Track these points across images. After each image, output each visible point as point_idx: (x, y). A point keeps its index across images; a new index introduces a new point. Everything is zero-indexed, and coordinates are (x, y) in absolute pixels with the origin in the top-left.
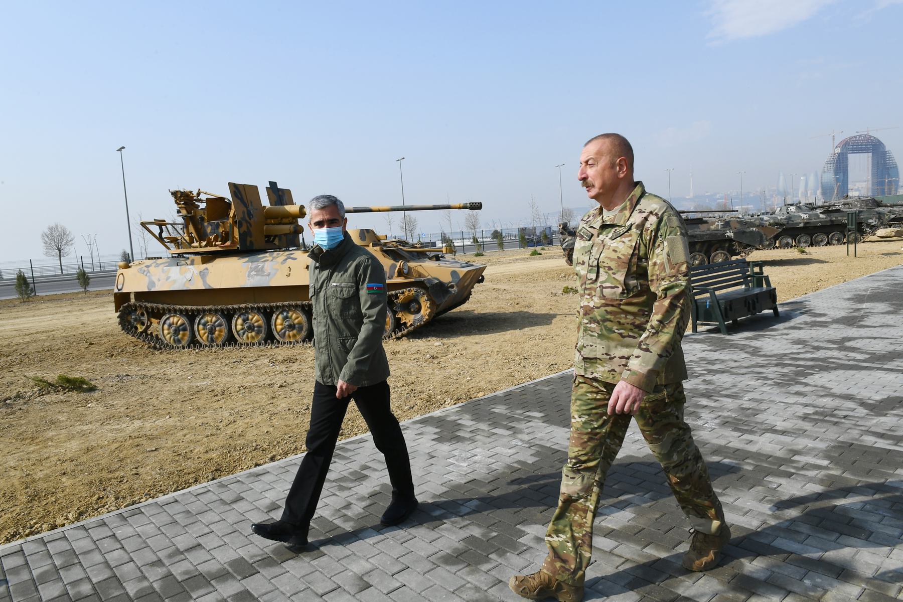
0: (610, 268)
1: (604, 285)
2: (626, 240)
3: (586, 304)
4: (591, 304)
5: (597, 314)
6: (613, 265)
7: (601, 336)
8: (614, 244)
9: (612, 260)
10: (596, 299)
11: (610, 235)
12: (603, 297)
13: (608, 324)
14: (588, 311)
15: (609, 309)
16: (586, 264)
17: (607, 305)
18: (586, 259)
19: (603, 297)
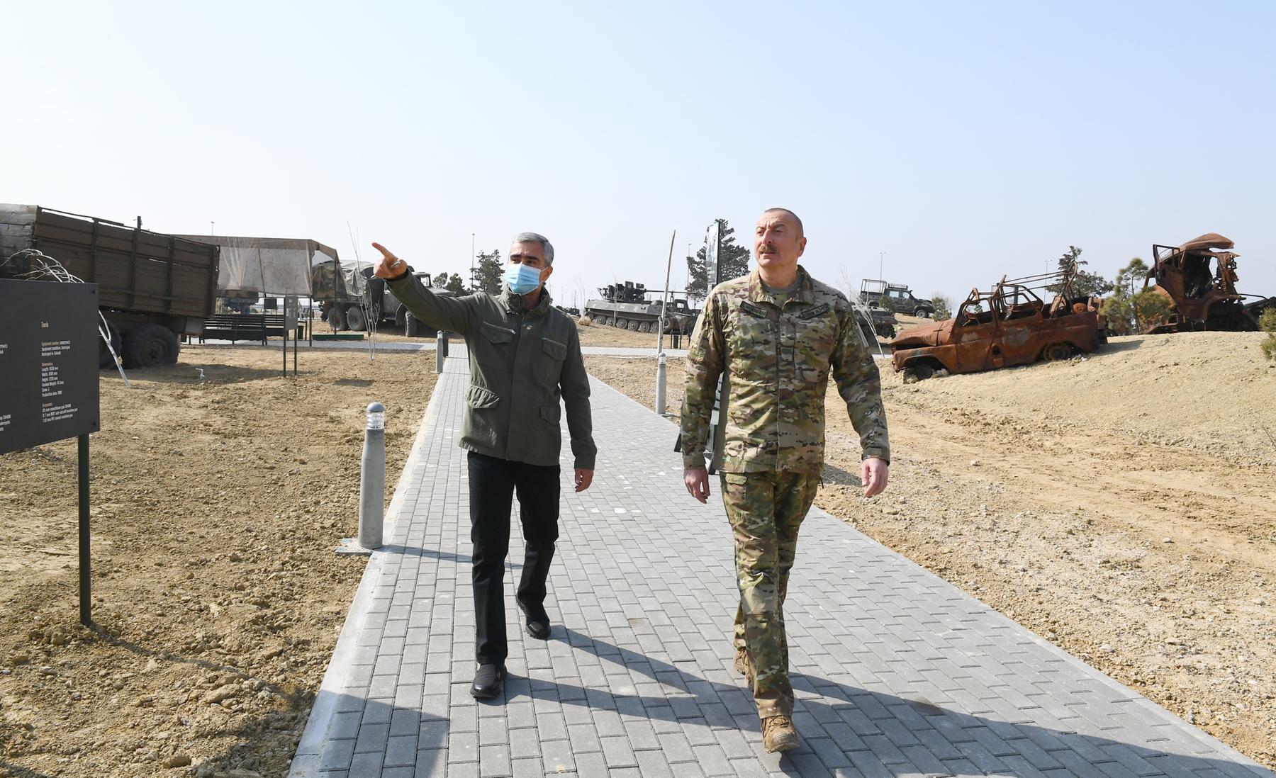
0: (812, 349)
1: (804, 367)
2: (826, 320)
3: (782, 387)
4: (791, 388)
5: (796, 399)
6: (816, 345)
7: (795, 423)
8: (812, 324)
9: (814, 340)
10: (796, 382)
11: (798, 314)
12: (803, 379)
13: (806, 408)
14: (784, 396)
15: (809, 392)
16: (773, 344)
17: (806, 388)
18: (771, 337)
19: (803, 379)
